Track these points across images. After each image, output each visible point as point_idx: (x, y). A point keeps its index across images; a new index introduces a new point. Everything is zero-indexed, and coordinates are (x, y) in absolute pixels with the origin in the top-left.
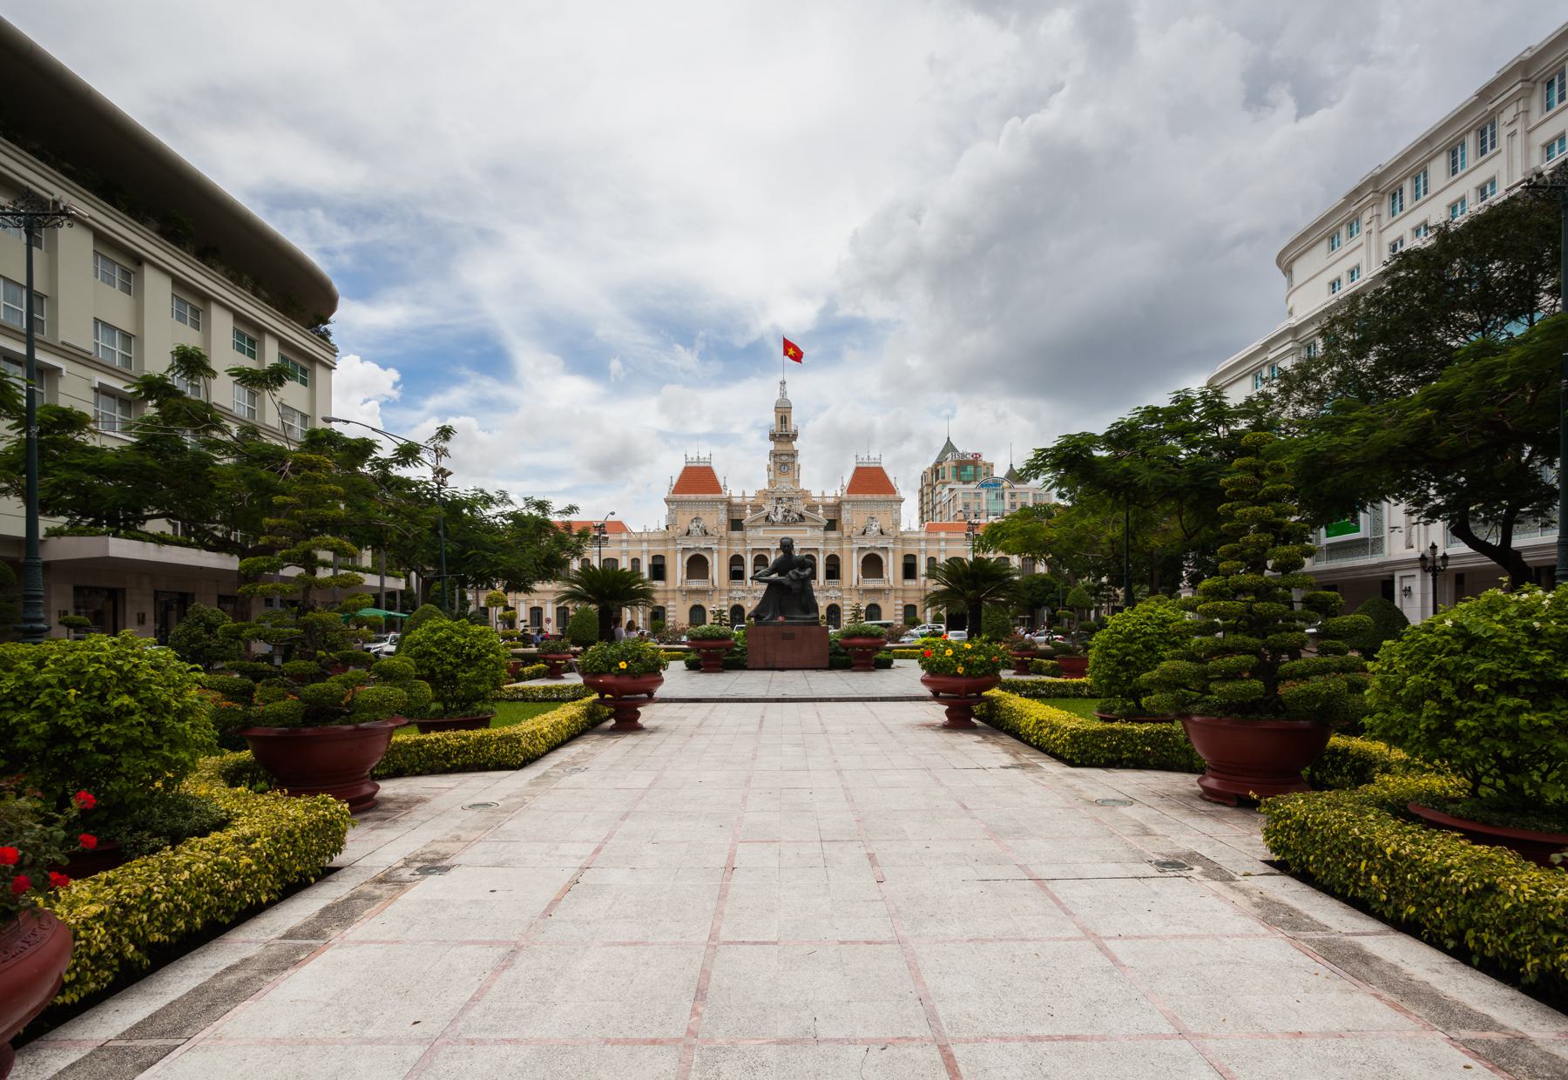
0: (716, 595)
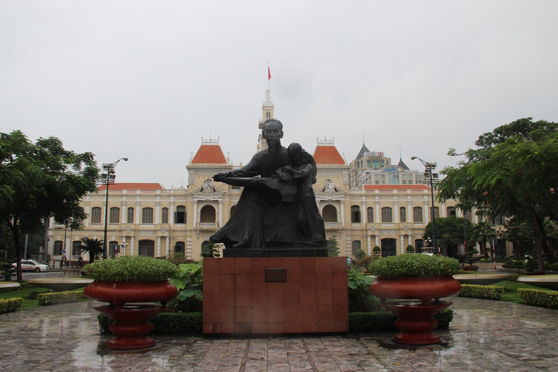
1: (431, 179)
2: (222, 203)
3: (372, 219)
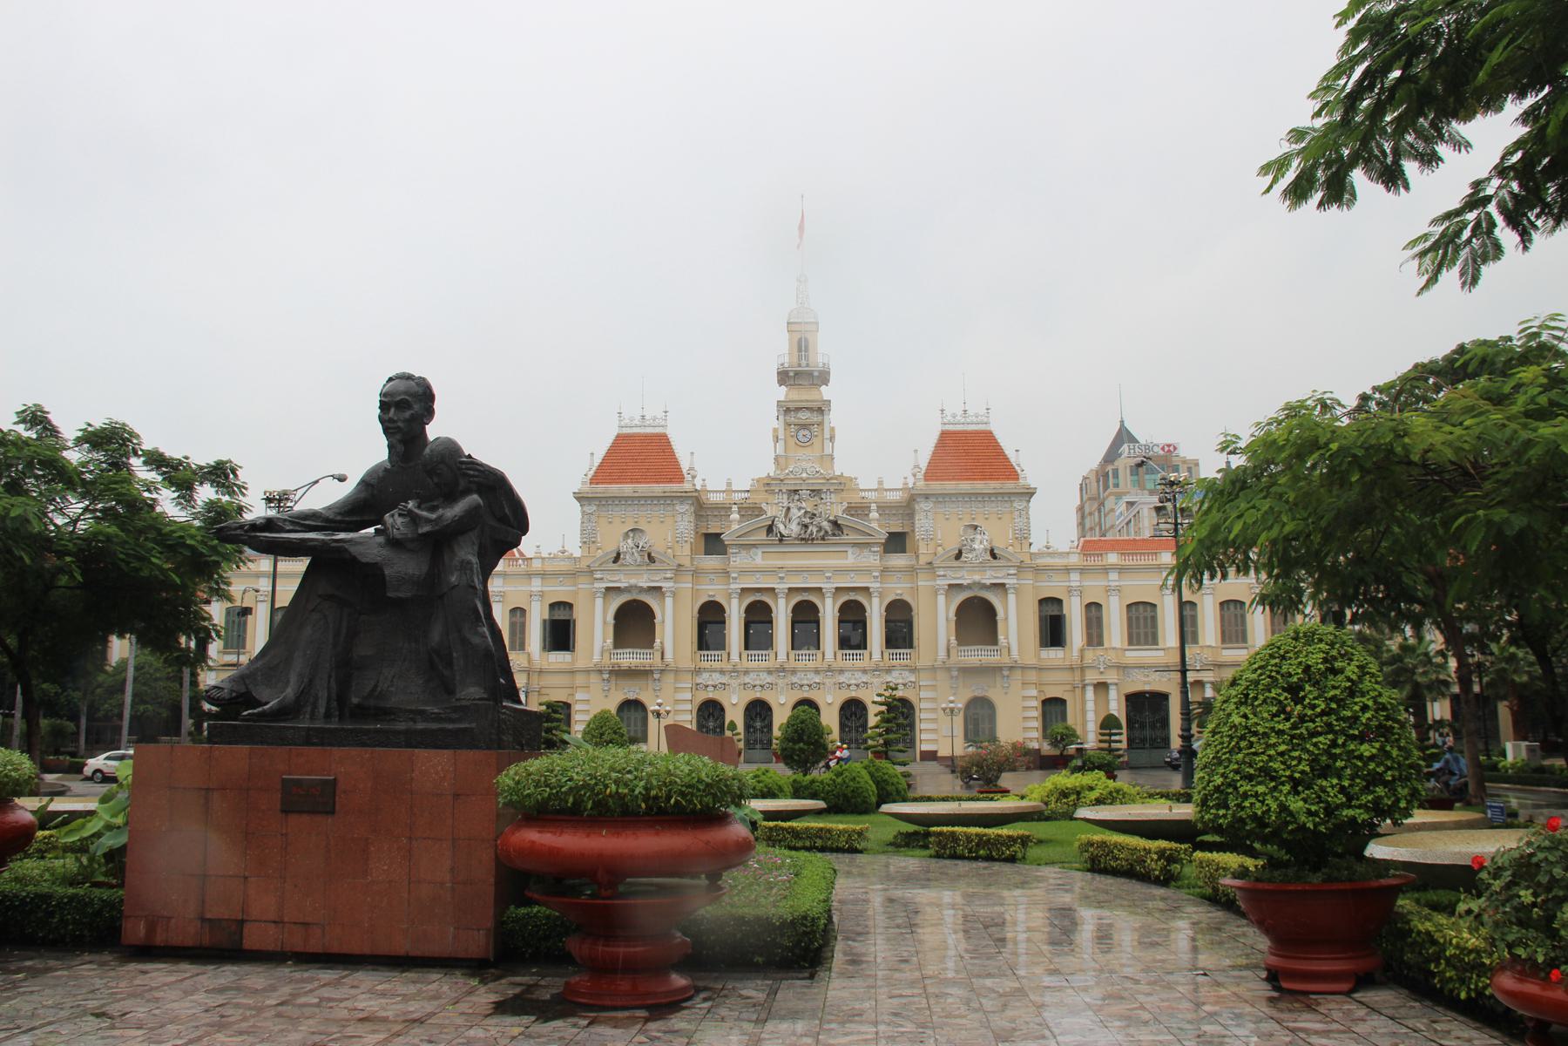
0: (669, 678)
1: (1176, 524)
2: (674, 594)
3: (1100, 636)
